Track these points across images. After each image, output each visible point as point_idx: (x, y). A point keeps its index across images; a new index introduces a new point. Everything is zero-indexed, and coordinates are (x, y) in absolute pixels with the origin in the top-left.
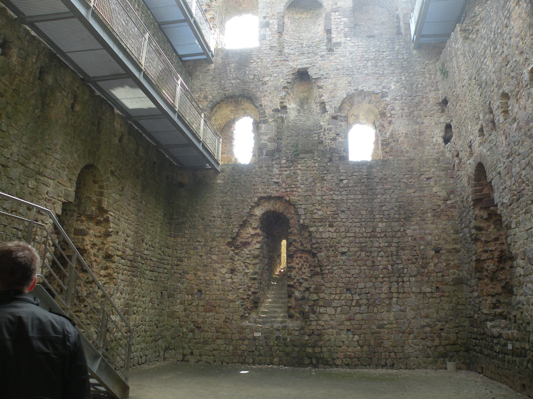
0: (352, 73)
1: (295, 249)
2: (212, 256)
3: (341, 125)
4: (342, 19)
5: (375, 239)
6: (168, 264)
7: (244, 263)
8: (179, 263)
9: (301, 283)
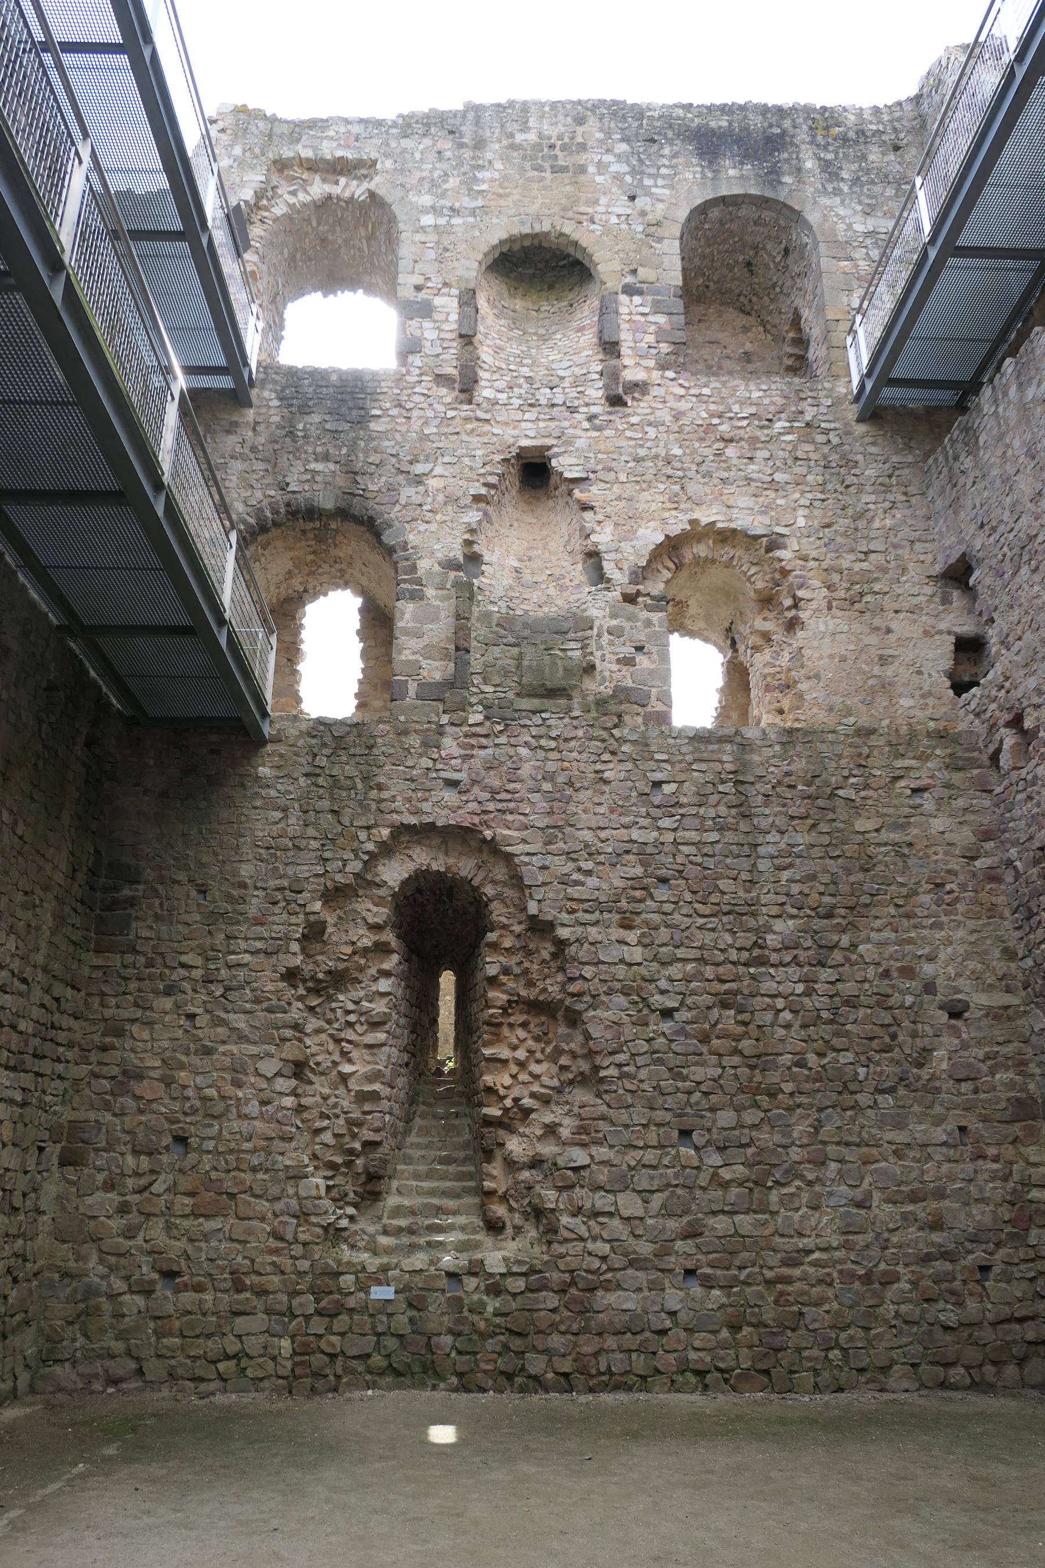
0: (680, 473)
1: (505, 997)
2: (232, 1016)
3: (648, 623)
4: (651, 318)
5: (763, 969)
6: (70, 1045)
7: (338, 1041)
8: (108, 1040)
9: (527, 1112)
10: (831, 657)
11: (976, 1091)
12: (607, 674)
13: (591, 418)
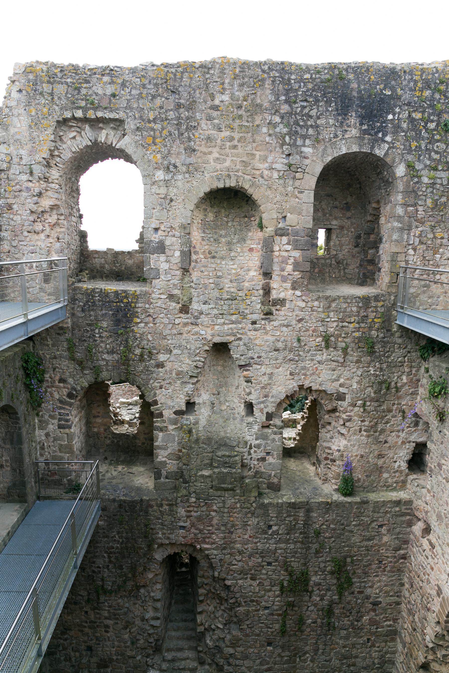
0: (297, 358)
3: (274, 440)
10: (357, 456)
11: (377, 628)
12: (252, 466)
13: (254, 323)
